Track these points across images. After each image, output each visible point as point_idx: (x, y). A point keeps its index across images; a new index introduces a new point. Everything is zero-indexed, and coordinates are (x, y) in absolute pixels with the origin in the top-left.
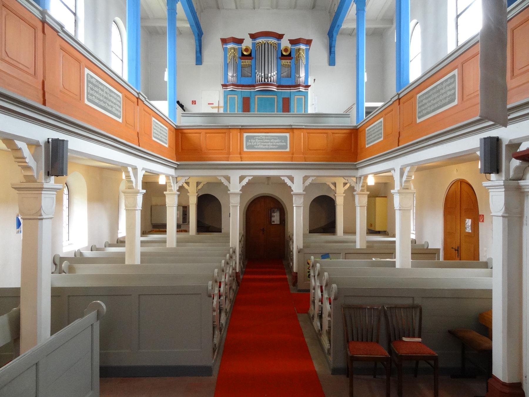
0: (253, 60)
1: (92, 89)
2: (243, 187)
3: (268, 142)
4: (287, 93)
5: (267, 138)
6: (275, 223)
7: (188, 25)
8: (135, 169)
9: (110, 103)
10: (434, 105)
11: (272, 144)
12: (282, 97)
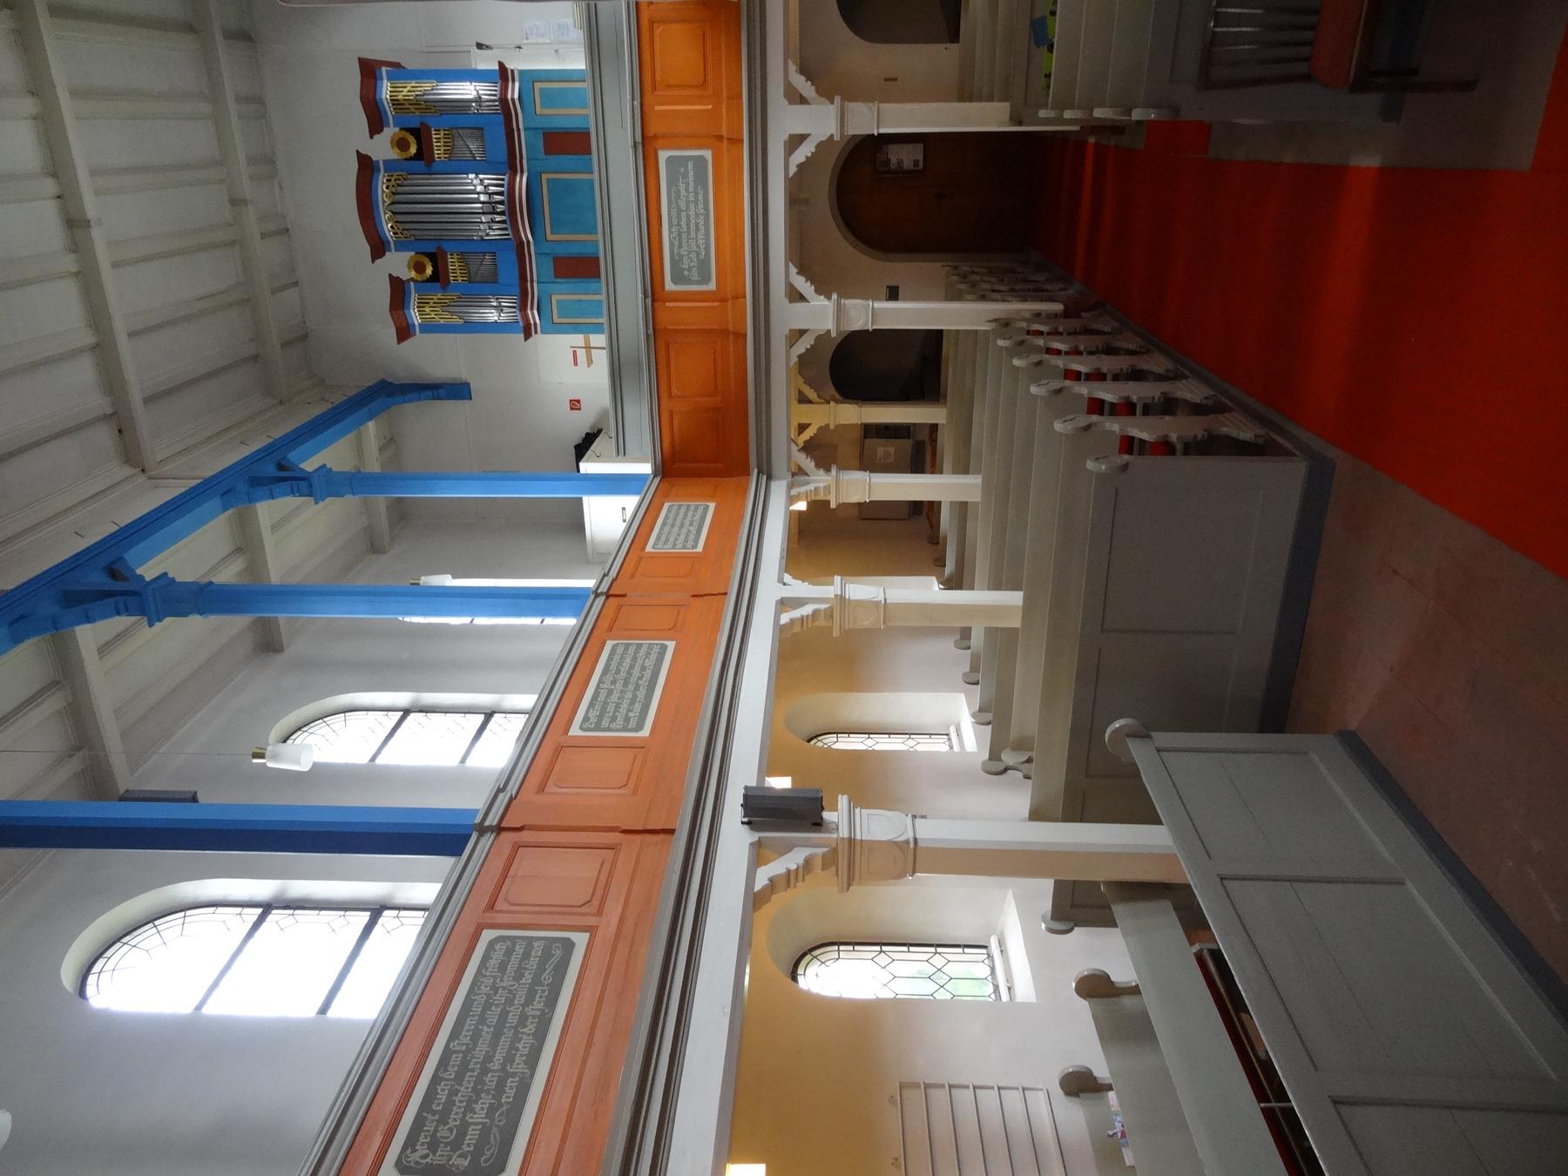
0: (445, 246)
1: (614, 719)
2: (818, 291)
3: (688, 216)
4: (534, 139)
5: (675, 221)
6: (921, 158)
7: (371, 424)
8: (784, 604)
9: (636, 673)
11: (692, 205)
12: (542, 156)
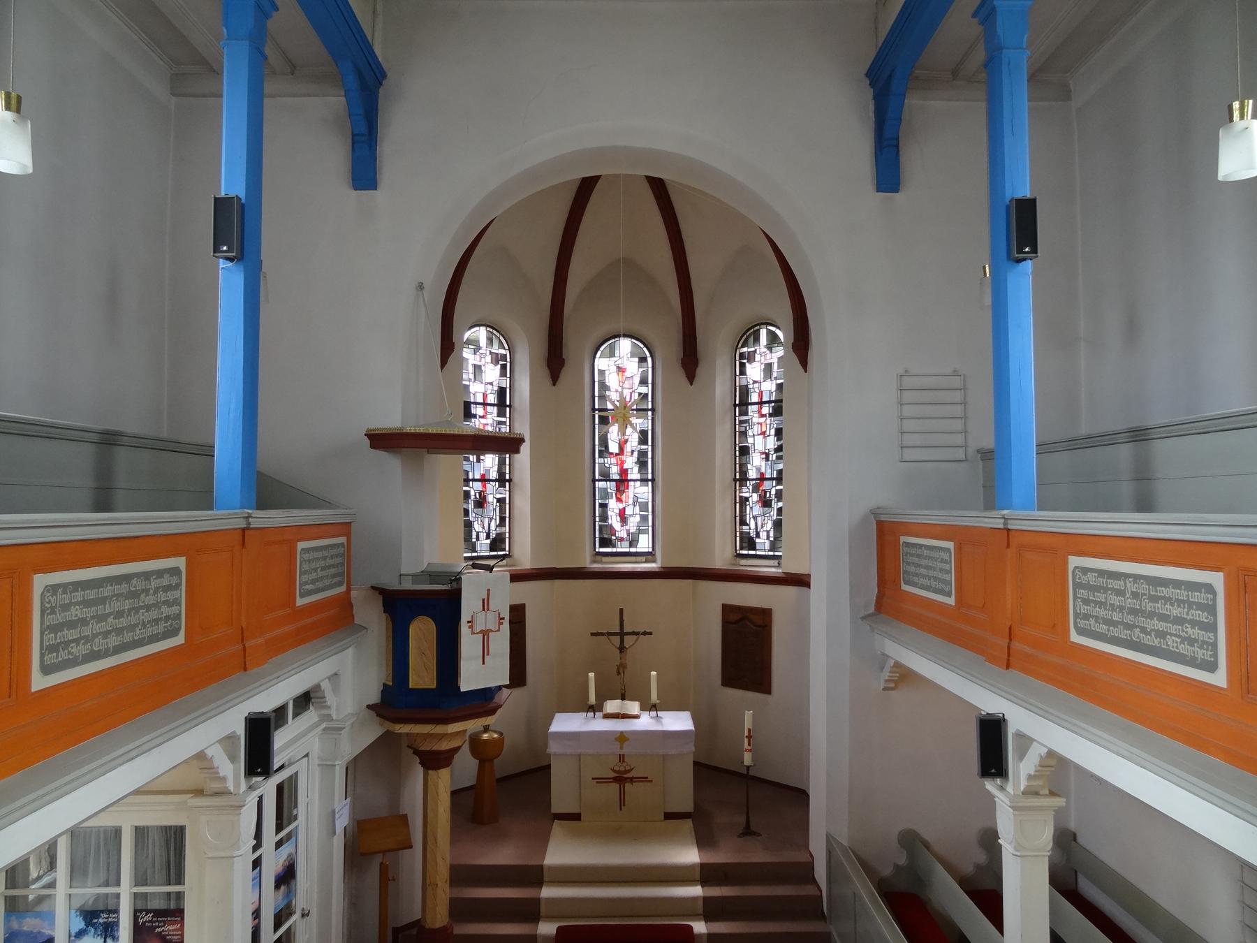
1: (1086, 602)
10: (119, 631)
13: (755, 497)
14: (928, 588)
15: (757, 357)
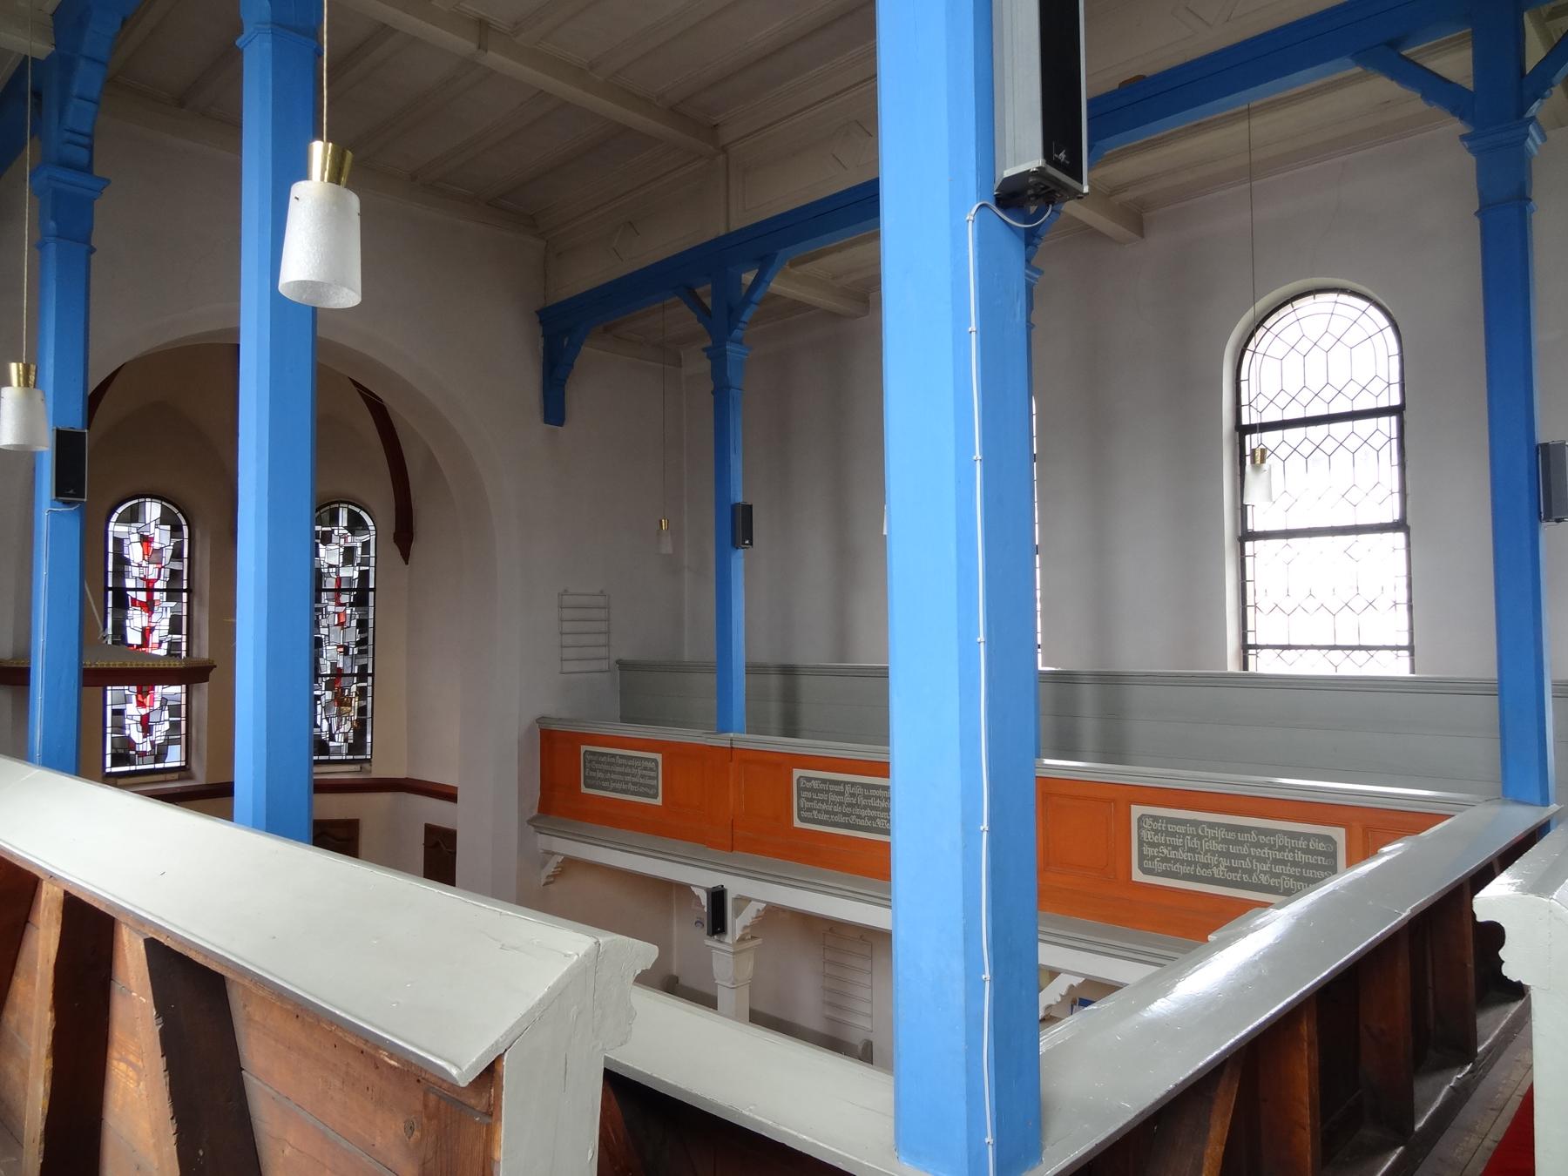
13: (329, 695)
14: (614, 790)
15: (335, 539)
